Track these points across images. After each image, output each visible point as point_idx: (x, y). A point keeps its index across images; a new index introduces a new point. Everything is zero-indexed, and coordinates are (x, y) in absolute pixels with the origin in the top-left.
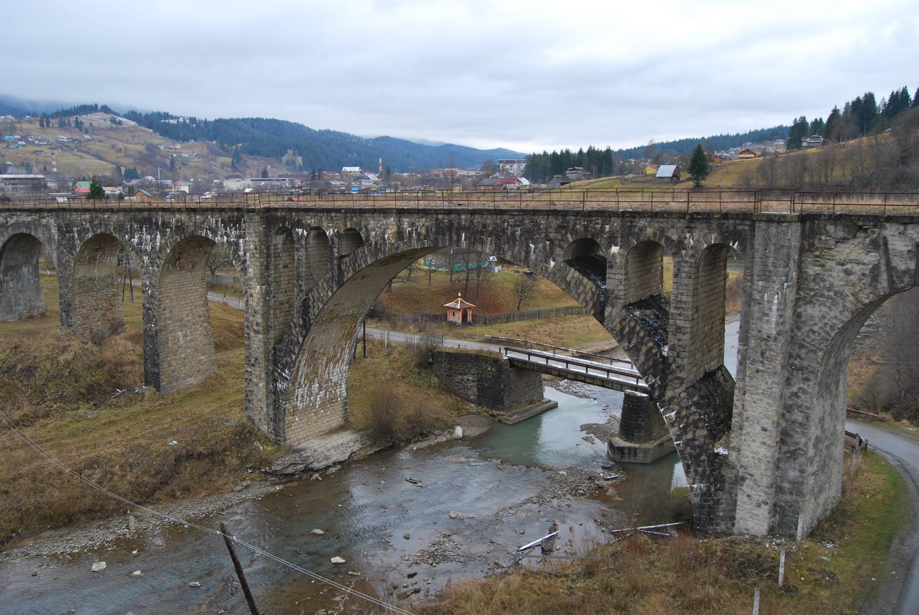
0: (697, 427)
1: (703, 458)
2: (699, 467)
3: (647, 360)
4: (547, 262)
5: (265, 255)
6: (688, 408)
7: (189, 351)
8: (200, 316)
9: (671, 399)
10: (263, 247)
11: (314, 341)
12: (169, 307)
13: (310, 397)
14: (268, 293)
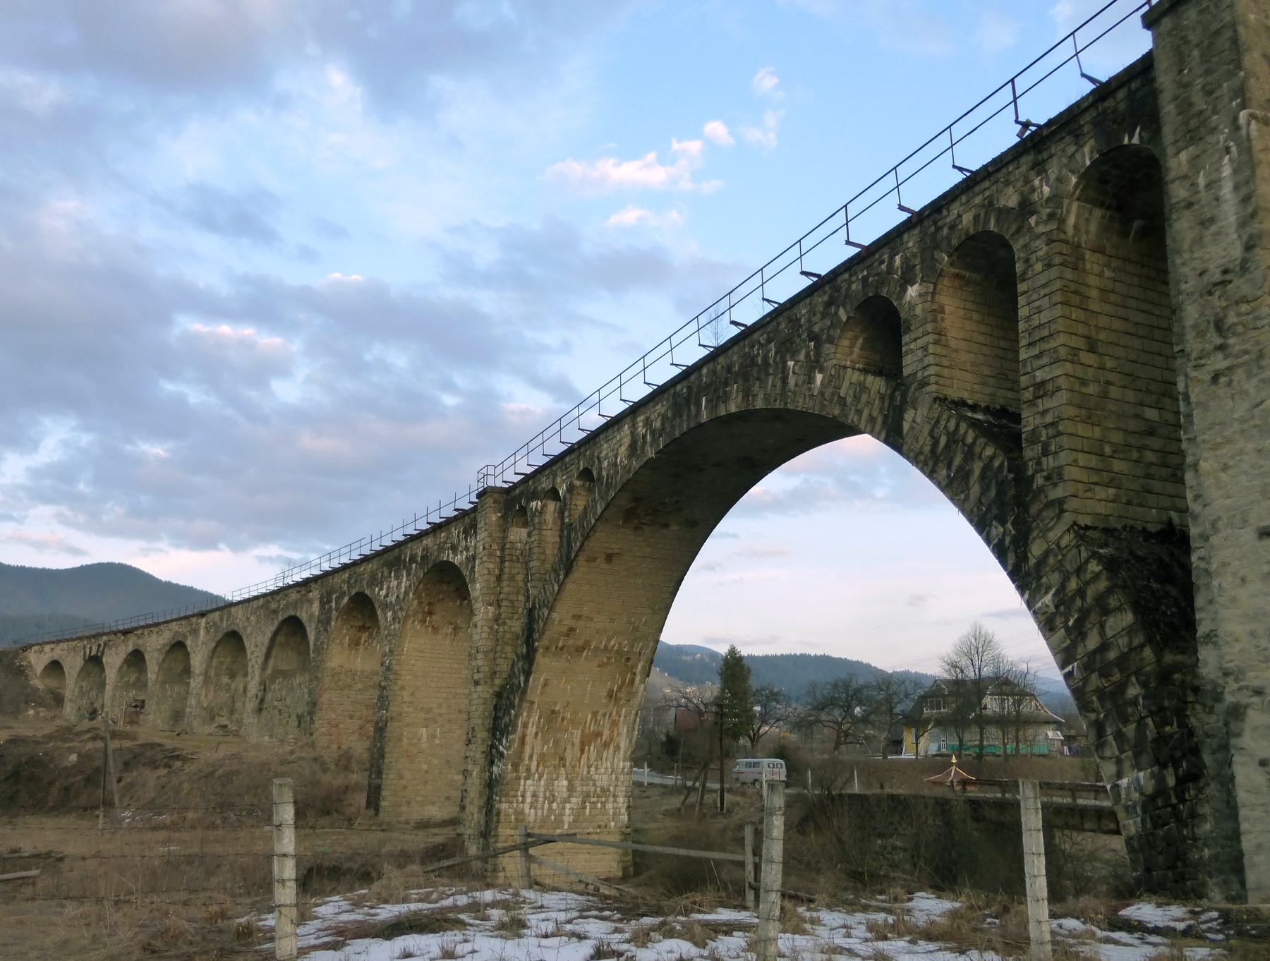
0: (1106, 612)
1: (1133, 691)
2: (1126, 722)
3: (985, 490)
4: (811, 380)
5: (498, 560)
6: (1080, 570)
7: (436, 761)
8: (460, 711)
9: (1042, 561)
10: (495, 546)
13: (551, 803)
14: (497, 619)
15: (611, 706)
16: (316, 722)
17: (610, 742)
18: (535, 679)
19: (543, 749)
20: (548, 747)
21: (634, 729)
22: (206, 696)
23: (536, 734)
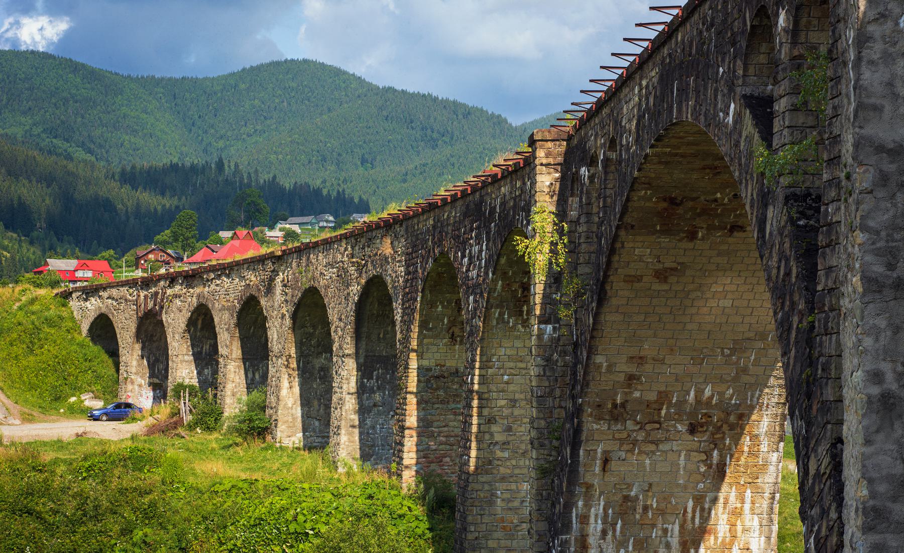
11: (613, 465)
17: (732, 543)
21: (771, 521)
23: (604, 533)
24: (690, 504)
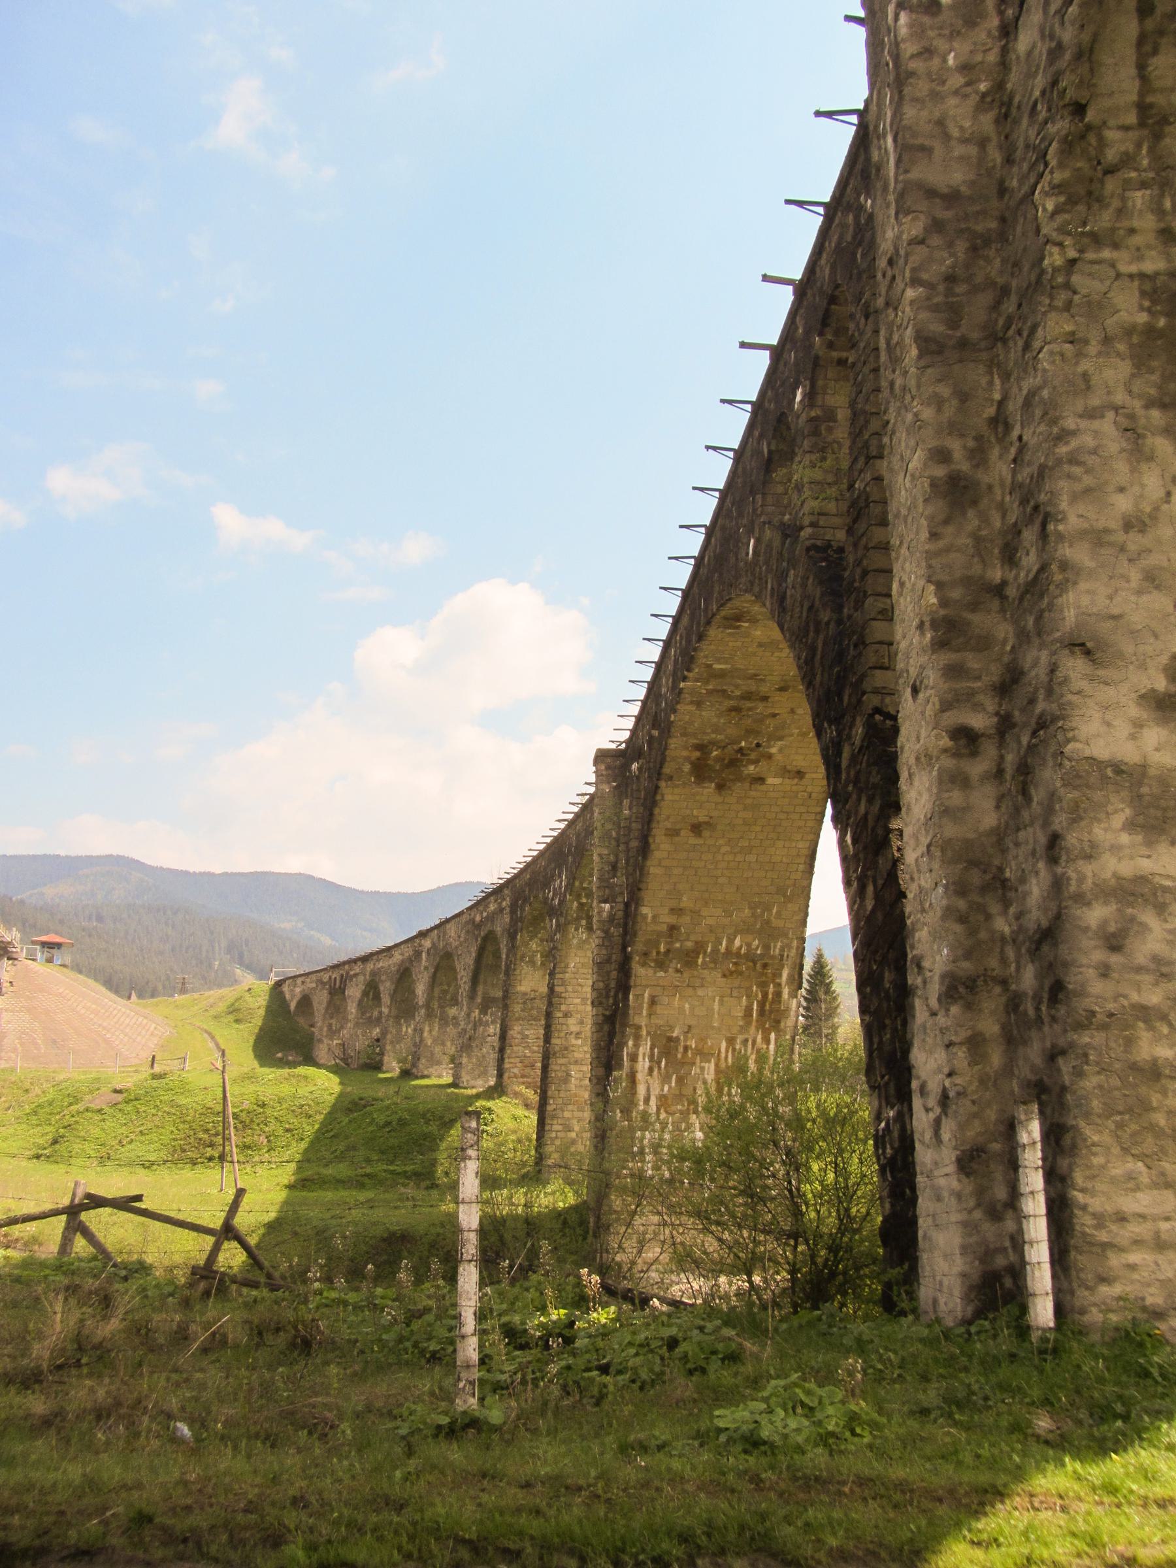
5: (614, 843)
11: (659, 1009)
12: (578, 1012)
15: (752, 1030)
16: (506, 1060)
18: (637, 996)
19: (662, 1090)
20: (670, 1087)
22: (430, 1031)
23: (651, 1070)
24: (724, 1045)
